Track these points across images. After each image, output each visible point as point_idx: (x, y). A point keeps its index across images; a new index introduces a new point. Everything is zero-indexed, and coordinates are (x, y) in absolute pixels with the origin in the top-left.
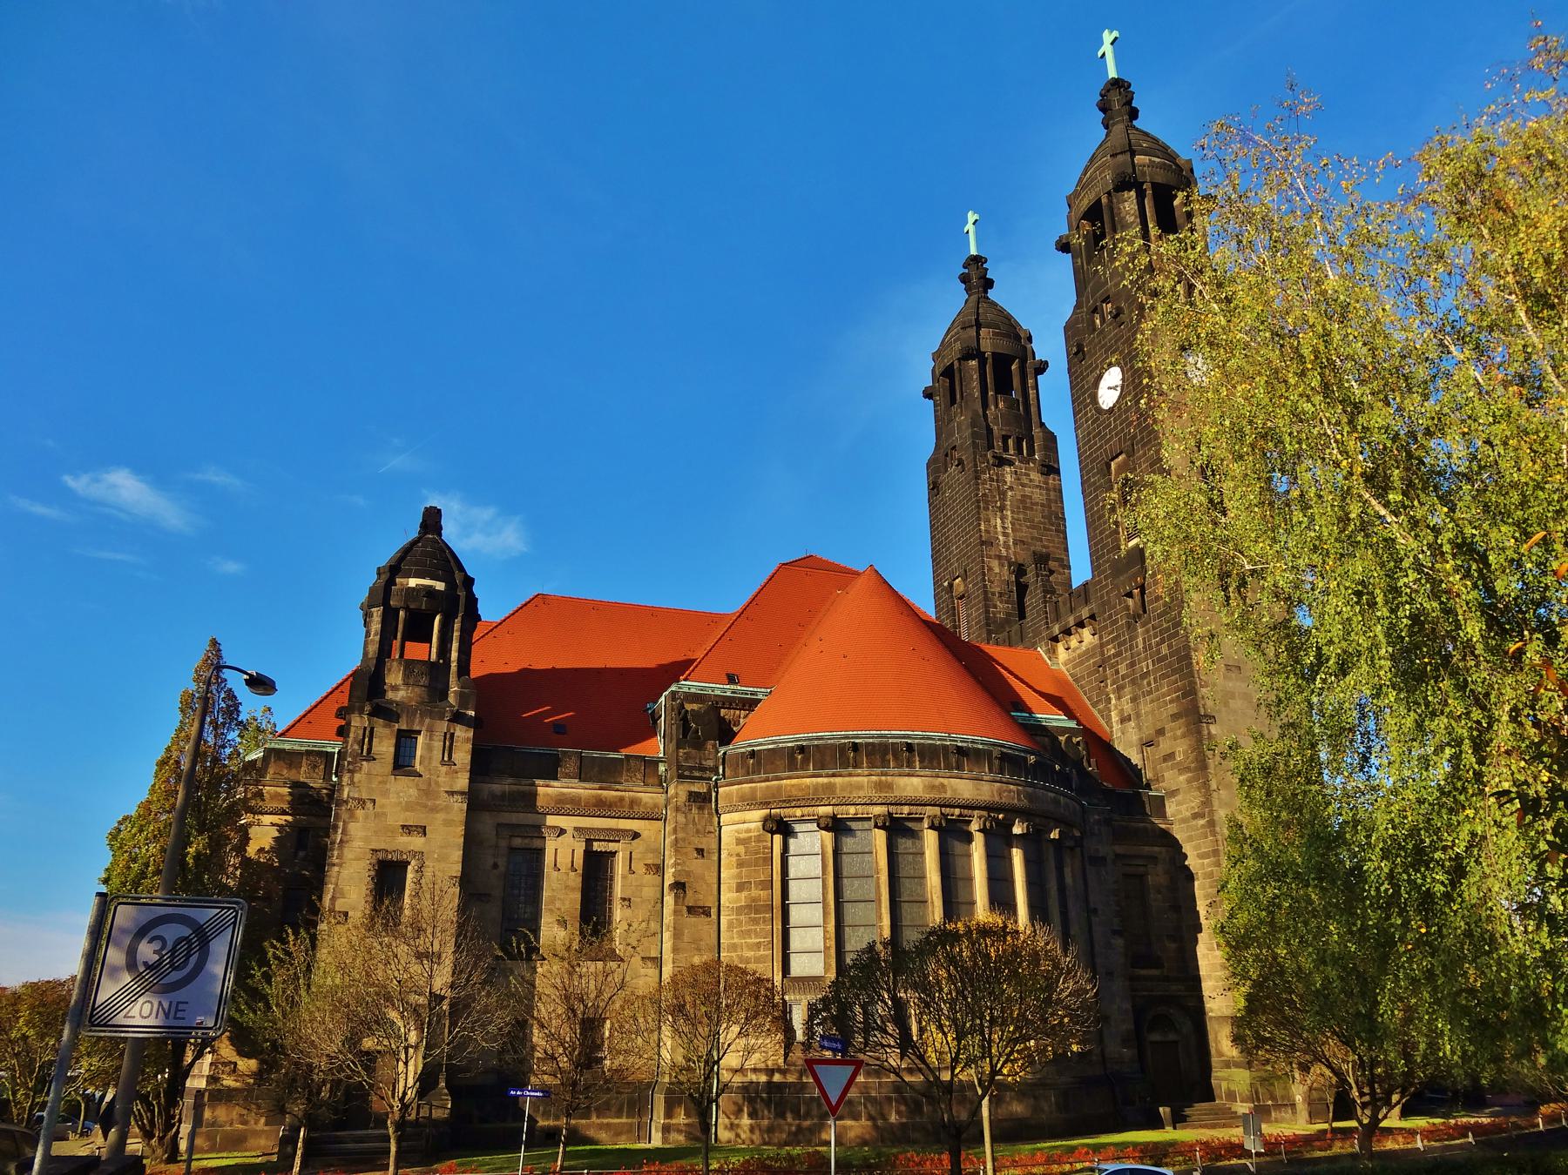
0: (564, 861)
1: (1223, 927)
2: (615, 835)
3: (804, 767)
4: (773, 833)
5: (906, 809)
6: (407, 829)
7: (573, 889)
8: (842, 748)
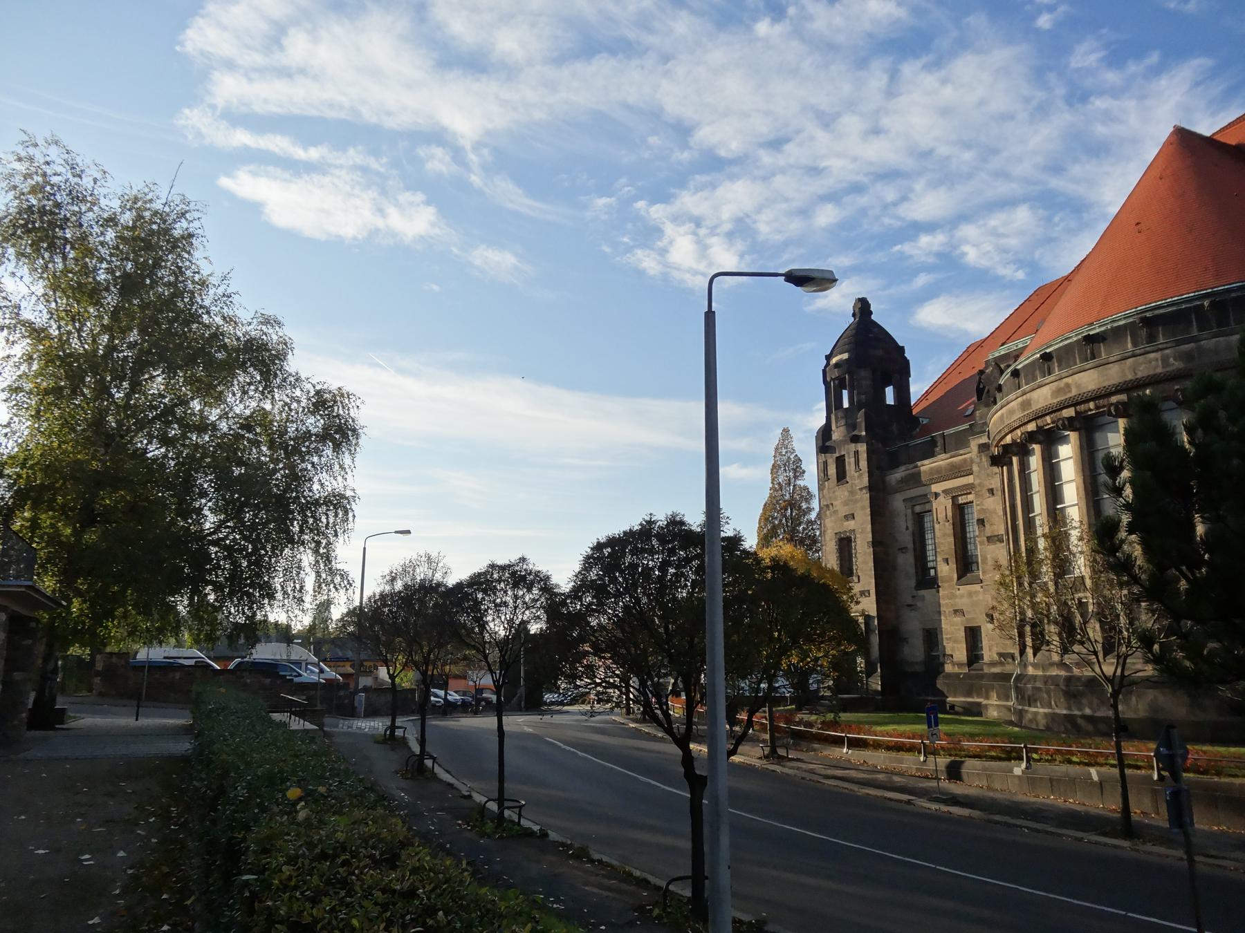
0: (941, 516)
2: (968, 489)
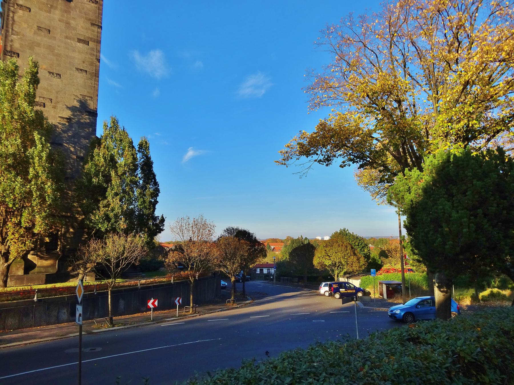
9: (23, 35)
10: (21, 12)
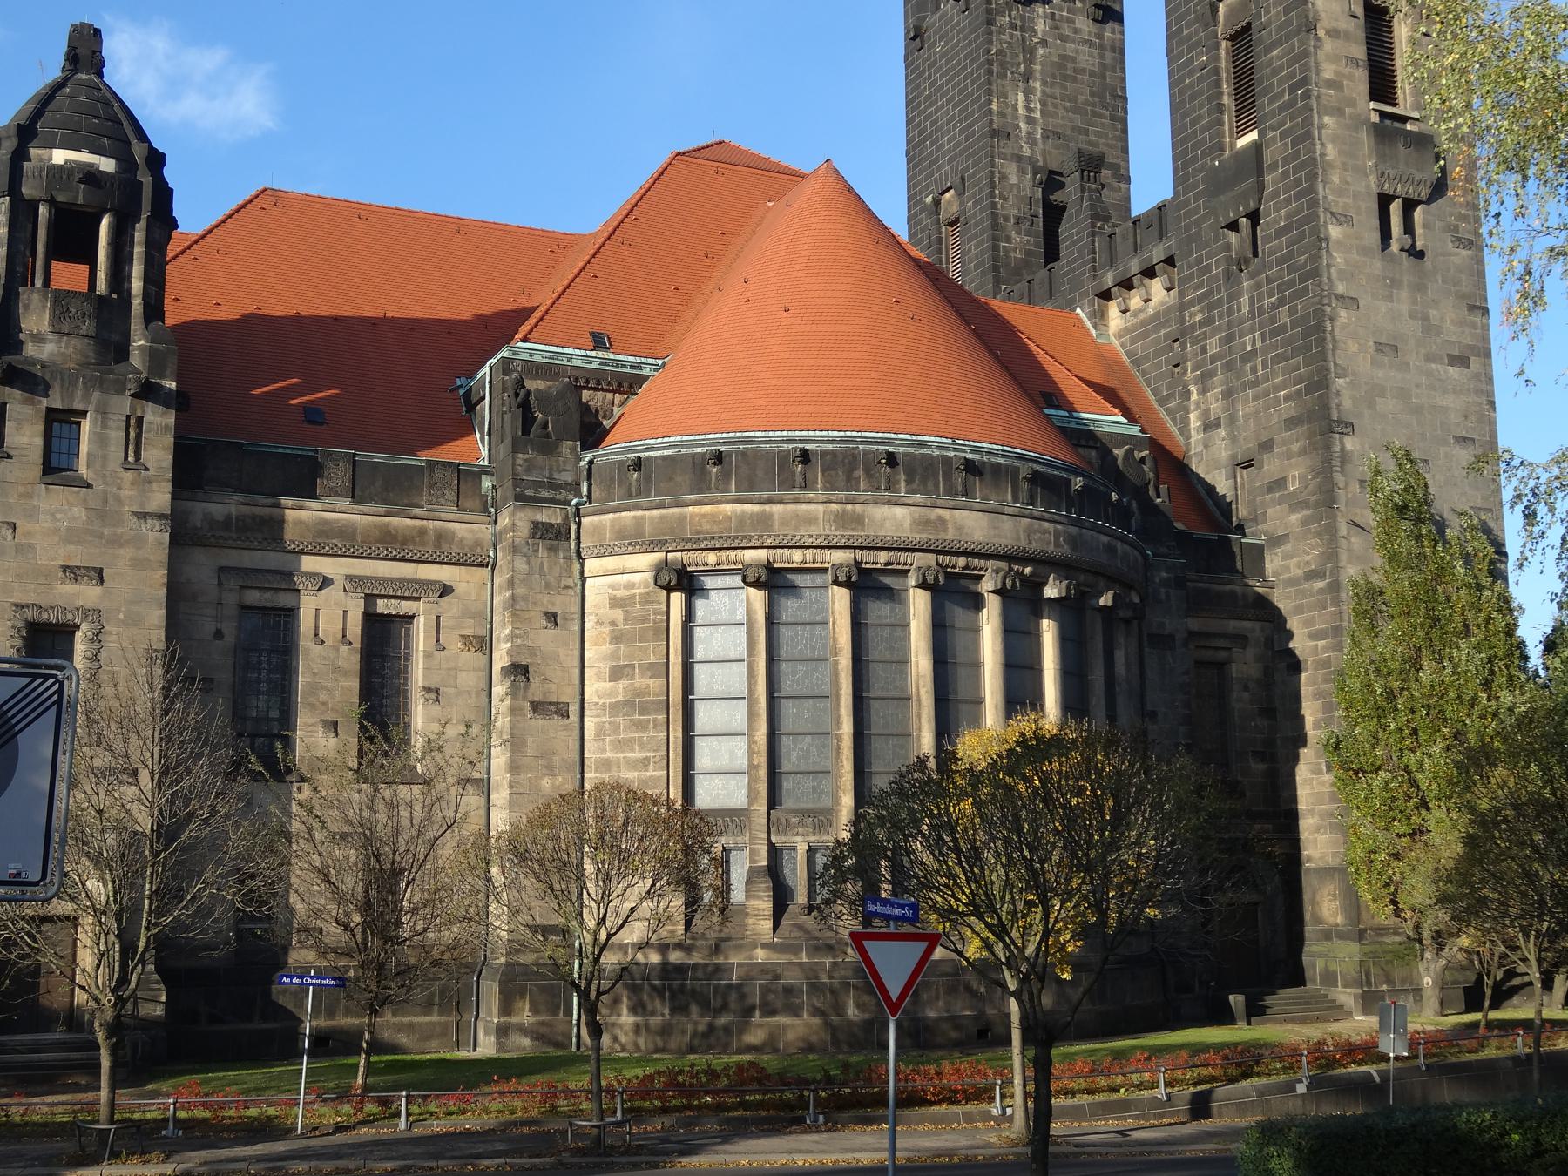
1: (1338, 743)
2: (413, 590)
3: (722, 485)
4: (669, 589)
5: (883, 557)
6: (72, 573)
7: (346, 674)
8: (784, 457)
9: (1354, 374)
10: (1343, 313)
